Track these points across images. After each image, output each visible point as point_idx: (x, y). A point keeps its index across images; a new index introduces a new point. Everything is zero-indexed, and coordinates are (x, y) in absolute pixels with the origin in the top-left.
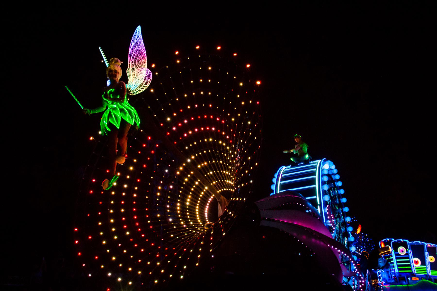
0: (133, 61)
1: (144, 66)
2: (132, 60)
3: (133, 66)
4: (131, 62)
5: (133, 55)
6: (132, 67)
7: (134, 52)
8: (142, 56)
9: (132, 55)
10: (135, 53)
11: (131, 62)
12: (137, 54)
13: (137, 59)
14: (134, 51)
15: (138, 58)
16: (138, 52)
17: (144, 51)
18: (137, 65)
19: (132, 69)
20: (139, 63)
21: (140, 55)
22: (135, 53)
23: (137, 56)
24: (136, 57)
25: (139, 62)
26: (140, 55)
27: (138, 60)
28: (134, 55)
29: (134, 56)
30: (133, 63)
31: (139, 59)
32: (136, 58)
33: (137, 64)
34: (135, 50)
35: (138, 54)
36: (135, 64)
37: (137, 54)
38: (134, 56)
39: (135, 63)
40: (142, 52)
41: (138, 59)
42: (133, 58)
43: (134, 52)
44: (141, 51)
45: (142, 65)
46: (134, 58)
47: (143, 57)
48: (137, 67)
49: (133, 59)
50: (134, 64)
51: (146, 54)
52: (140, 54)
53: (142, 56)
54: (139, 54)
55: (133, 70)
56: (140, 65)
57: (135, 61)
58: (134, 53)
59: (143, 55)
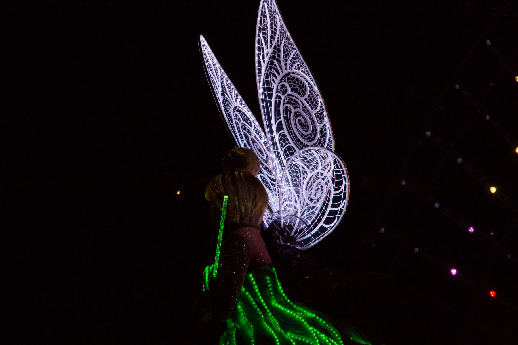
0: (280, 124)
1: (321, 132)
2: (276, 122)
3: (284, 141)
4: (274, 127)
5: (276, 102)
6: (282, 145)
7: (275, 90)
8: (306, 96)
9: (270, 102)
10: (278, 94)
11: (274, 127)
12: (286, 95)
13: (291, 112)
14: (275, 86)
15: (295, 108)
16: (289, 89)
17: (308, 78)
18: (297, 134)
19: (285, 151)
20: (302, 125)
21: (299, 97)
22: (278, 94)
23: (289, 103)
24: (285, 105)
25: (303, 122)
26: (299, 94)
27: (297, 117)
28: (280, 102)
29: (278, 104)
30: (283, 129)
31: (300, 110)
32: (287, 111)
33: (298, 131)
34: (277, 82)
35: (289, 92)
36: (291, 133)
37: (286, 95)
38: (279, 106)
39: (289, 128)
40: (301, 82)
41: (293, 111)
42: (277, 113)
43: (275, 90)
44: (298, 80)
45: (314, 129)
46: (279, 110)
47: (311, 99)
48: (298, 140)
49: (279, 115)
50: (286, 131)
51: (316, 88)
52: (296, 92)
53: (306, 96)
54: (293, 93)
55: (287, 156)
56: (307, 131)
57: (287, 120)
58: (277, 92)
59: (308, 93)
